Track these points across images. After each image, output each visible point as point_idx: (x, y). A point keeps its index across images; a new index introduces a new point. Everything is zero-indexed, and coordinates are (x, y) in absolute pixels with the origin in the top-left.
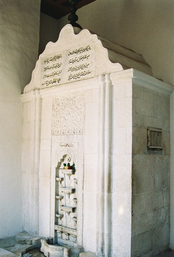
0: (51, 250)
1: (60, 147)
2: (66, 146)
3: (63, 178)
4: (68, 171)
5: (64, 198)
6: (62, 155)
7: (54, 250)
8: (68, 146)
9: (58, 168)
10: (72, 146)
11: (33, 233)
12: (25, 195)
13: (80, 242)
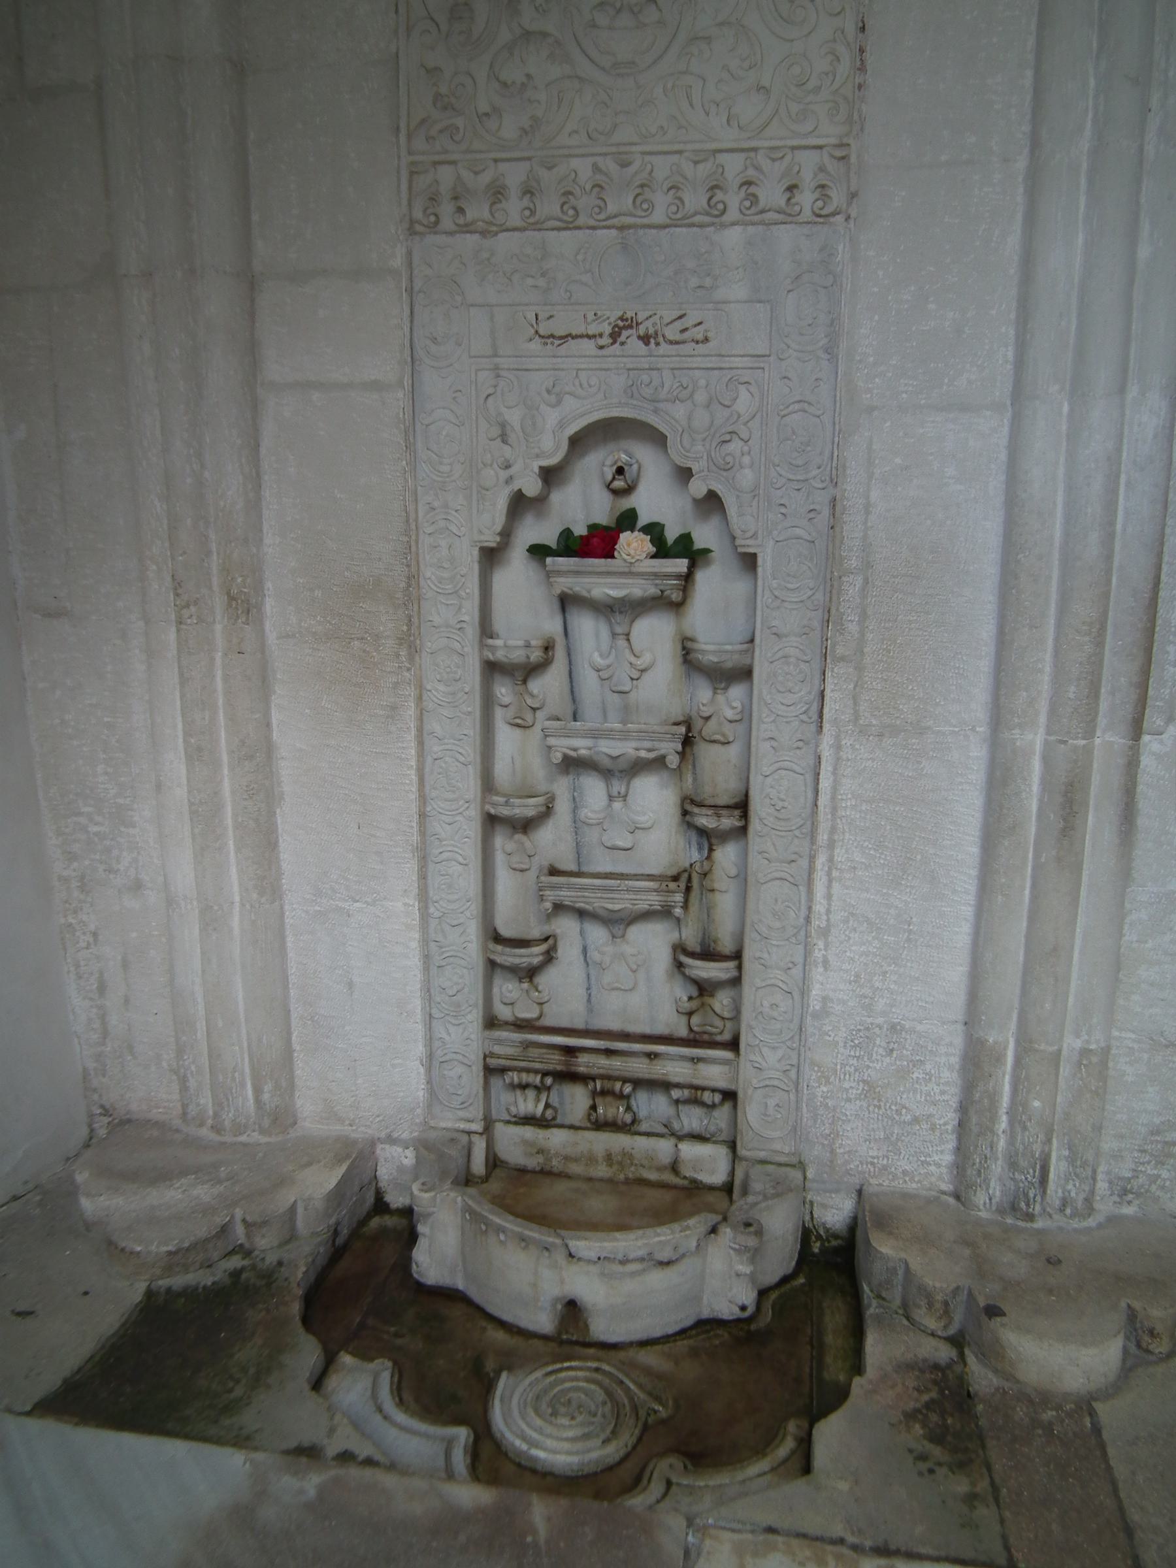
0: (602, 1274)
1: (536, 345)
2: (615, 336)
3: (554, 641)
5: (562, 807)
6: (561, 425)
7: (633, 1274)
8: (645, 339)
9: (491, 557)
10: (698, 333)
11: (239, 1129)
12: (82, 820)
13: (777, 1134)
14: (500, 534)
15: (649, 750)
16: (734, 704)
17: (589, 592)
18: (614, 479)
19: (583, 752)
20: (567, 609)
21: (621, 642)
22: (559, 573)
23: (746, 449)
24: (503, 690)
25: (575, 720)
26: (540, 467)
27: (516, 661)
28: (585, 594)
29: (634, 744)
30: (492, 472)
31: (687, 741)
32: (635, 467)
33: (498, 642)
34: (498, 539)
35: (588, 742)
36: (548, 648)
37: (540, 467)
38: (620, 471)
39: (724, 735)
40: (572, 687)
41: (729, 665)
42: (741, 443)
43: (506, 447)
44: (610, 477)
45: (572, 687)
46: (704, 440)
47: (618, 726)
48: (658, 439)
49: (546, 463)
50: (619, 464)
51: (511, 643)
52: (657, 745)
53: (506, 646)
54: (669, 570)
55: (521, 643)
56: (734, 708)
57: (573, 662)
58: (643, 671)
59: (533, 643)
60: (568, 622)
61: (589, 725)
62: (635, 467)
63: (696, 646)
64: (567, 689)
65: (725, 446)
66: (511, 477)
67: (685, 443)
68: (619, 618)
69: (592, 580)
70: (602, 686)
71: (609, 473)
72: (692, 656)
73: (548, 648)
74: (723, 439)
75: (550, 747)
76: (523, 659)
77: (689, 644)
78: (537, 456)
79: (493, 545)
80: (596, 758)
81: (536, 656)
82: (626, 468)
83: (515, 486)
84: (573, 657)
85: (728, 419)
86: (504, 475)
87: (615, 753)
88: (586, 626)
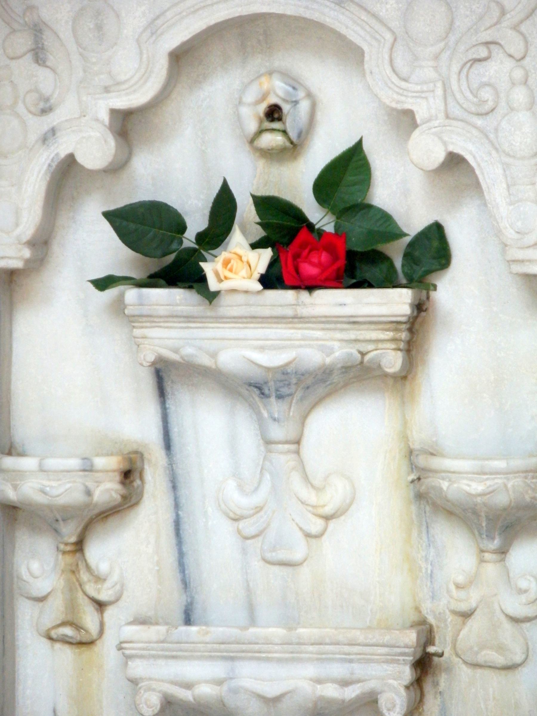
4: (297, 319)
14: (32, 244)
15: (345, 683)
16: (523, 584)
17: (214, 355)
18: (260, 132)
19: (206, 691)
20: (168, 389)
21: (283, 460)
22: (151, 319)
23: (518, 74)
24: (35, 566)
25: (188, 621)
26: (114, 112)
27: (62, 501)
28: (205, 361)
29: (311, 670)
30: (15, 123)
31: (424, 665)
32: (304, 106)
33: (28, 463)
34: (27, 253)
35: (217, 669)
36: (128, 475)
37: (114, 112)
38: (274, 113)
39: (501, 649)
40: (181, 555)
41: (502, 500)
42: (509, 64)
43: (42, 73)
44: (252, 126)
45: (181, 555)
46: (437, 57)
47: (277, 632)
48: (350, 54)
49: (122, 102)
50: (273, 100)
51: (52, 463)
52: (359, 670)
53: (42, 470)
54: (375, 310)
55: (74, 463)
56: (522, 591)
57: (183, 501)
58: (327, 518)
59: (100, 462)
60: (173, 419)
61: (218, 632)
62: (304, 106)
63: (436, 463)
64: (170, 558)
65: (478, 68)
66: (53, 131)
67: (399, 62)
68: (276, 407)
69: (220, 333)
70: (244, 551)
71: (251, 118)
72: (431, 481)
73: (128, 475)
74: (472, 55)
75: (134, 682)
76: (76, 497)
77: (421, 461)
78: (107, 90)
79: (17, 264)
80: (232, 702)
81: (107, 490)
82: (286, 108)
83: (63, 148)
84: (183, 492)
85: (481, 18)
86: (39, 125)
87: (271, 690)
88: (213, 429)
